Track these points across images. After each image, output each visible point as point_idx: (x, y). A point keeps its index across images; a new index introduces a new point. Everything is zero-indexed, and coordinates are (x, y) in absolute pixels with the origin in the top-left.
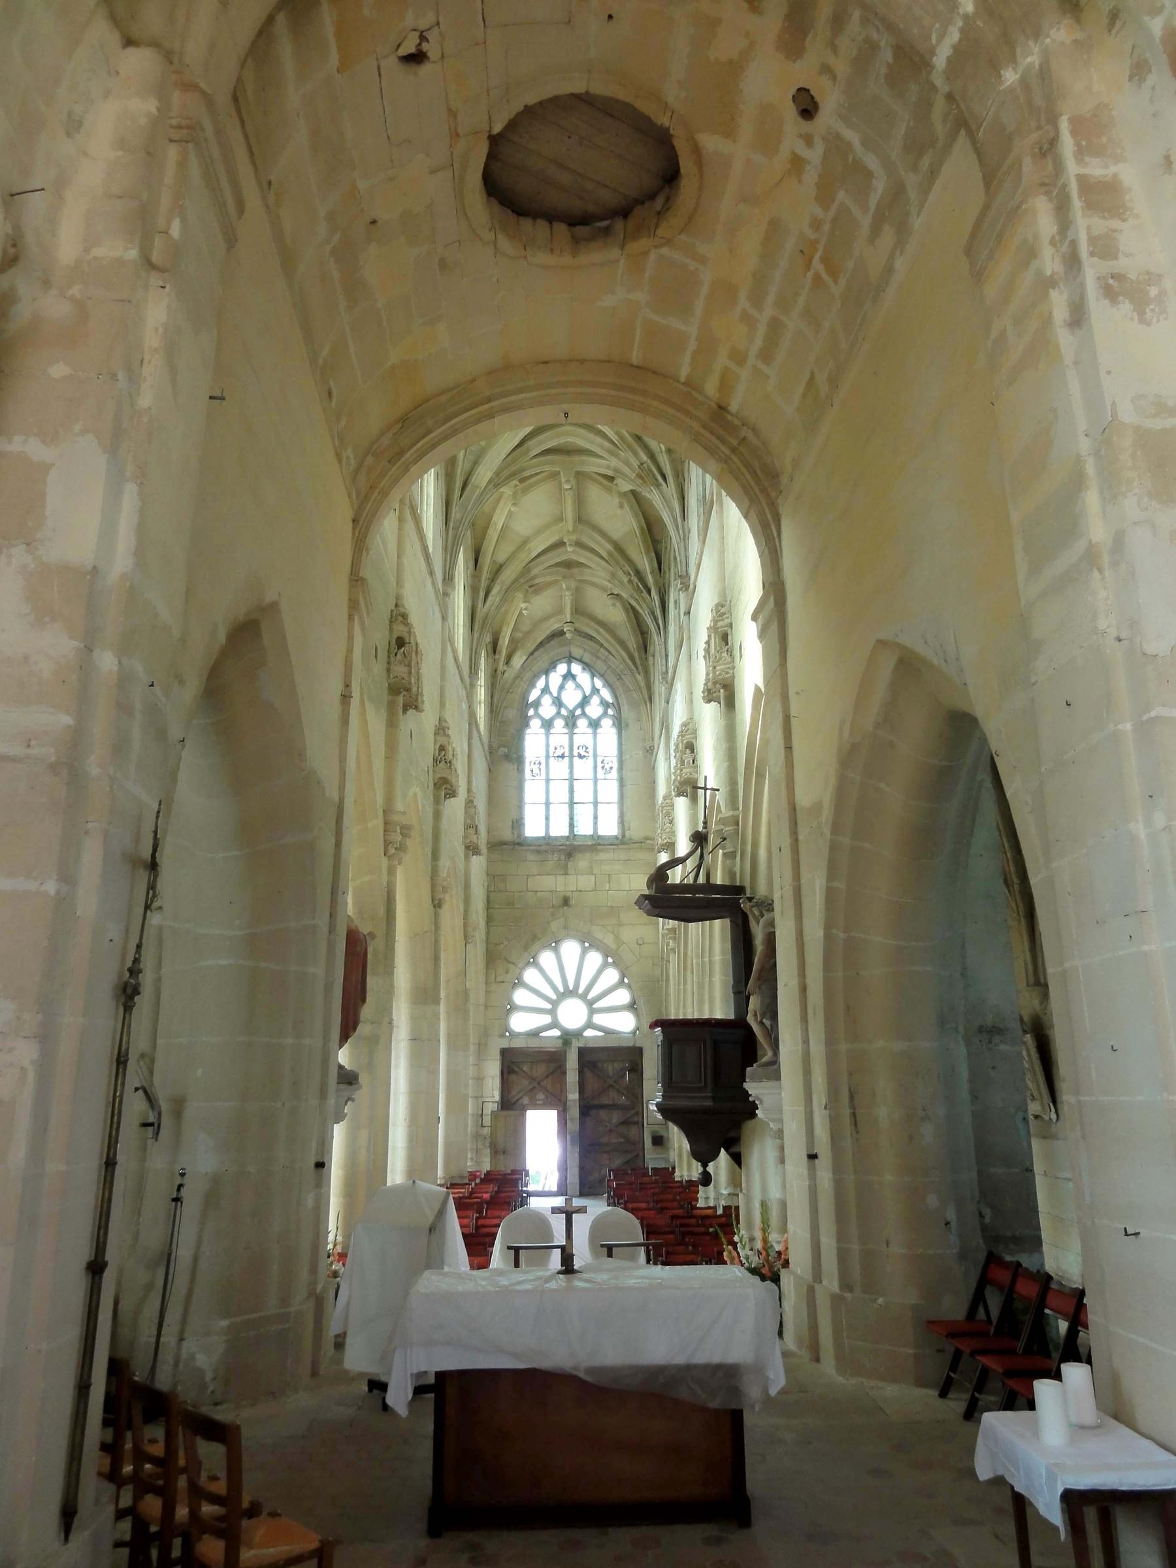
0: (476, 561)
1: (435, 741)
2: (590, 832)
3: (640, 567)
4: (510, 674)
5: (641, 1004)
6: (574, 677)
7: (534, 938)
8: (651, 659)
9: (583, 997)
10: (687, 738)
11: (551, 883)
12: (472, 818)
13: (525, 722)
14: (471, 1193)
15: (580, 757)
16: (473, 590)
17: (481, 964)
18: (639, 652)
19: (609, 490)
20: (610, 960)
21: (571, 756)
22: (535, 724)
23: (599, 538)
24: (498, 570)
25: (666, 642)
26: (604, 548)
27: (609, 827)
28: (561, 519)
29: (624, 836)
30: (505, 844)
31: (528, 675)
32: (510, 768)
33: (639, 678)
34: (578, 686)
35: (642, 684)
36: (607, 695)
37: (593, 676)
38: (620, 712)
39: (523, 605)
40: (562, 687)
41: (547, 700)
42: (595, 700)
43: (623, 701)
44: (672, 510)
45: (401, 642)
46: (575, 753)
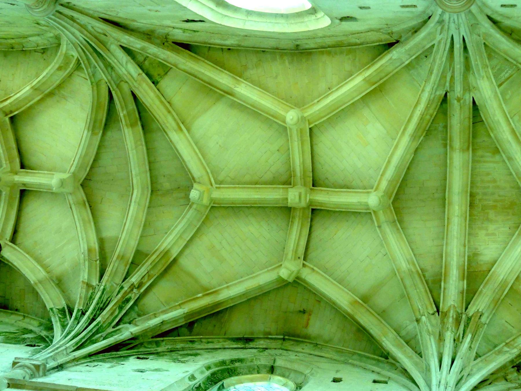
3: (150, 301)
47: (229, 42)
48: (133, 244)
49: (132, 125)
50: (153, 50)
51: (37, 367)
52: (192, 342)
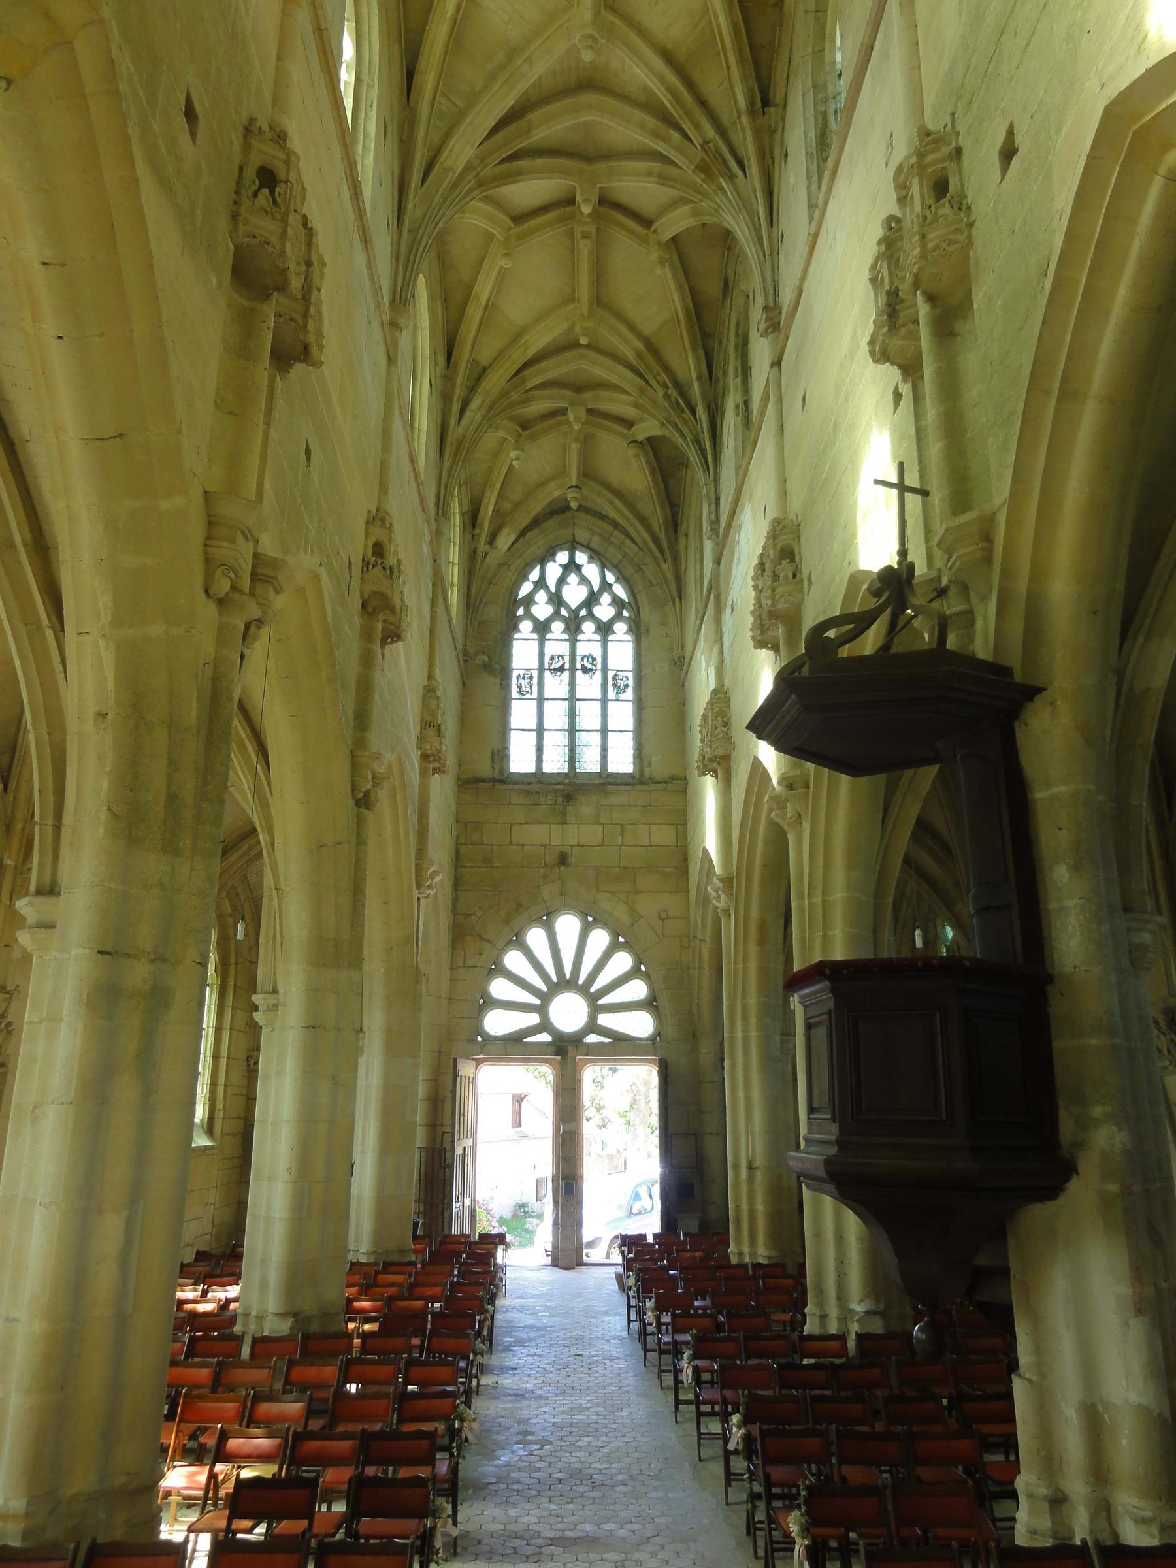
0: (449, 355)
1: (367, 533)
2: (596, 768)
3: (681, 374)
4: (492, 560)
5: (664, 1000)
6: (578, 568)
7: (520, 907)
8: (682, 540)
9: (584, 990)
11: (542, 835)
12: (433, 714)
13: (513, 625)
14: (412, 1286)
15: (585, 670)
16: (444, 397)
17: (445, 939)
18: (666, 528)
19: (643, 241)
20: (621, 940)
21: (573, 670)
22: (526, 626)
23: (624, 330)
24: (480, 374)
25: (716, 480)
26: (629, 347)
27: (622, 761)
28: (572, 299)
29: (642, 775)
30: (483, 780)
31: (519, 563)
32: (490, 681)
33: (665, 567)
34: (584, 580)
35: (670, 575)
36: (620, 591)
37: (603, 568)
39: (513, 454)
40: (562, 581)
41: (541, 597)
42: (606, 598)
43: (643, 598)
44: (753, 215)
45: (268, 178)
46: (579, 666)
47: (439, 309)
48: (630, 375)
49: (523, 382)
52: (721, 343)
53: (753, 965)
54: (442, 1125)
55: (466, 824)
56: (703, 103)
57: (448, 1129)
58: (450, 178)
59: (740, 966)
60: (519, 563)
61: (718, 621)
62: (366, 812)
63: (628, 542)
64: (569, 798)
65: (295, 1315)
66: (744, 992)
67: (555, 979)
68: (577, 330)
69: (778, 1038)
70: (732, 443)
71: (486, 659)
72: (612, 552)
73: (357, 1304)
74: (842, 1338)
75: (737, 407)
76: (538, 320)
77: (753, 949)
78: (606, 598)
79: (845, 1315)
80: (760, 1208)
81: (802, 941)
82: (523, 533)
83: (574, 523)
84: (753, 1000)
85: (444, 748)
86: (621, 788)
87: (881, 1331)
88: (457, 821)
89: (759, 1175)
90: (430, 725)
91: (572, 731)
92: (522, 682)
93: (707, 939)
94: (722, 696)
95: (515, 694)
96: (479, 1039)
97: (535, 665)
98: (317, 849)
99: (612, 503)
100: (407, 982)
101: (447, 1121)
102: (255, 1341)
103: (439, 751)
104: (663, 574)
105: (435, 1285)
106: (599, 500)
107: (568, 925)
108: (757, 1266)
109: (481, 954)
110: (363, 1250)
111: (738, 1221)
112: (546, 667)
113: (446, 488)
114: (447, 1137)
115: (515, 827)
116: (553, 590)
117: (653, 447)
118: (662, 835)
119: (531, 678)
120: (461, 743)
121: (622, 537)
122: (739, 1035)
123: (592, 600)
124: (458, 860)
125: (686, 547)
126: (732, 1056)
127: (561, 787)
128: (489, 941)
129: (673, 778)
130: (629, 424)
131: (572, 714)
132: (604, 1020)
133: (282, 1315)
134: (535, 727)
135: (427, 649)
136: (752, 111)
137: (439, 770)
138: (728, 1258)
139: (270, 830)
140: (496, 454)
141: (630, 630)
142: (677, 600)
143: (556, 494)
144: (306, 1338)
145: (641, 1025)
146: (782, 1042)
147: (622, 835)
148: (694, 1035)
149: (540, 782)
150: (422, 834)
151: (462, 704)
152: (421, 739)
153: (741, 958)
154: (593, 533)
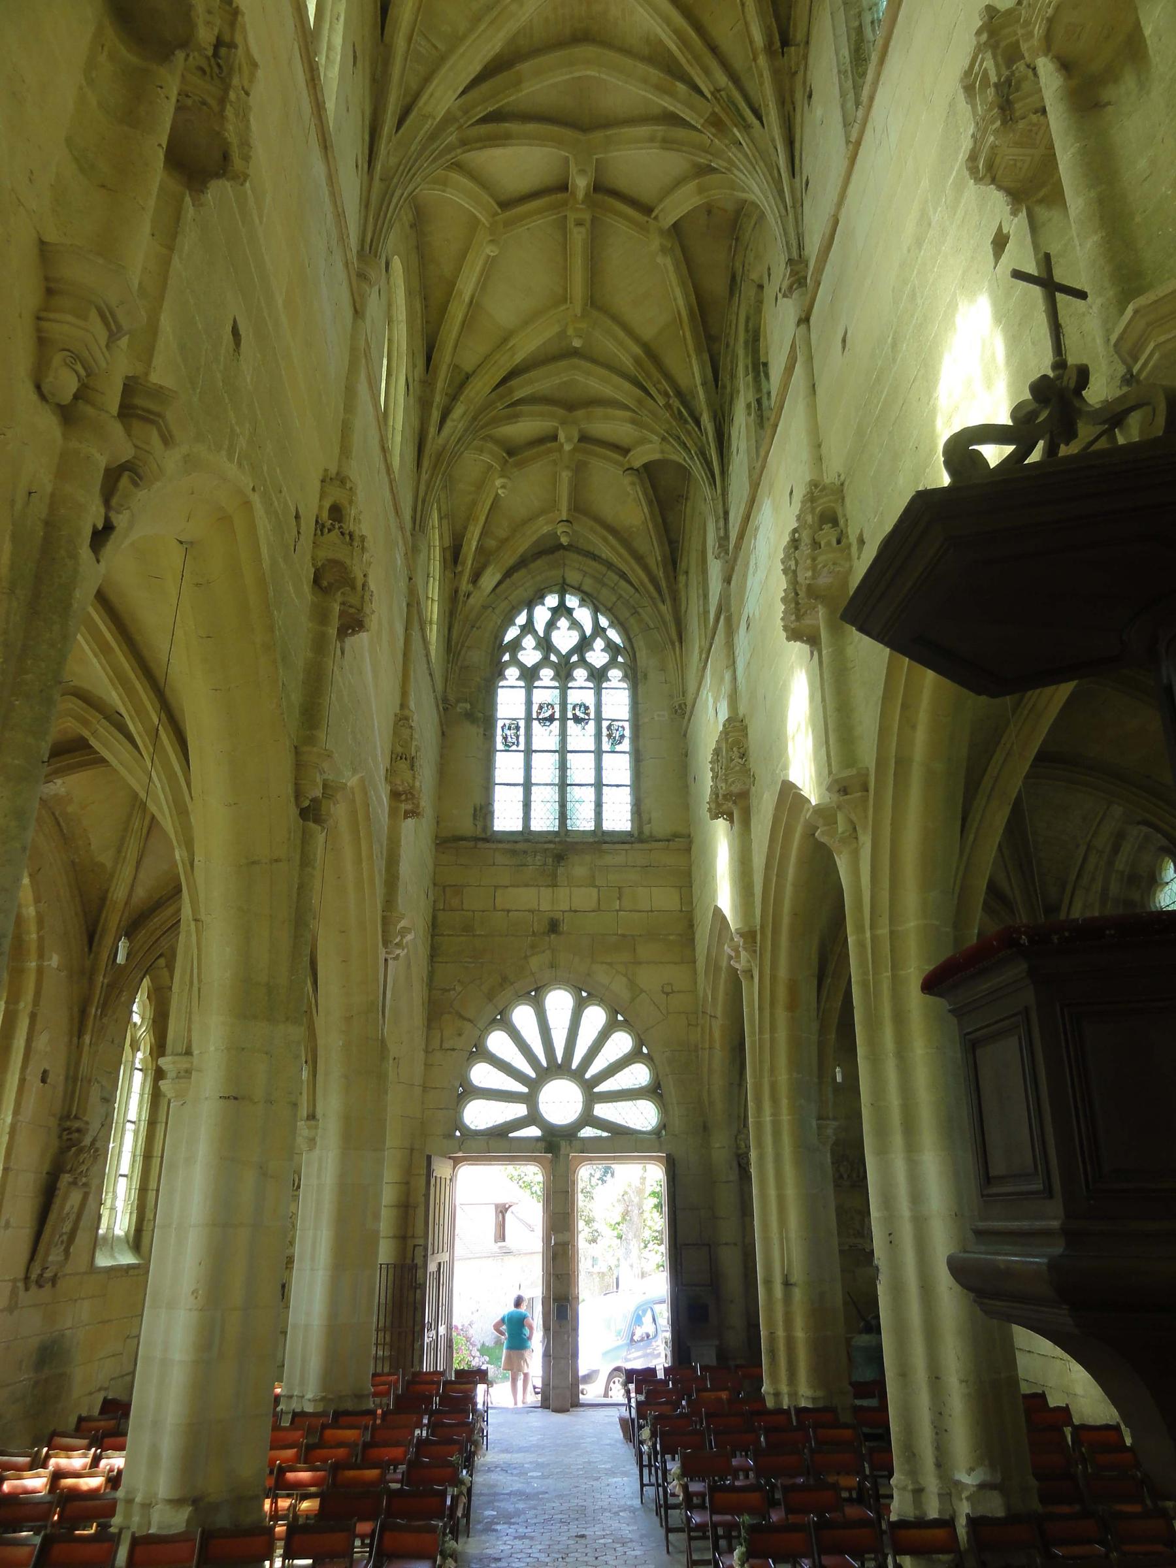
0: (429, 359)
1: (323, 495)
2: (590, 826)
3: (683, 382)
4: (476, 600)
6: (569, 612)
7: (504, 981)
8: (682, 579)
9: (577, 1076)
10: (822, 504)
11: (530, 899)
15: (577, 720)
17: (419, 1019)
18: (665, 567)
19: (643, 228)
20: (620, 1018)
21: (564, 720)
22: (512, 673)
23: (621, 334)
24: (461, 382)
25: (724, 494)
26: (626, 354)
27: (618, 818)
28: (565, 300)
29: (641, 832)
31: (504, 605)
32: (473, 731)
33: (663, 608)
34: (575, 625)
35: (669, 618)
36: (614, 635)
37: (596, 611)
38: (634, 658)
39: (498, 482)
40: (551, 625)
41: (529, 642)
42: (599, 644)
43: (640, 643)
44: (772, 168)
46: (570, 715)
47: (418, 306)
48: (627, 385)
49: (511, 391)
50: (437, 399)
51: (720, 546)
53: (782, 1035)
54: (413, 1237)
55: (444, 887)
56: (714, 49)
57: (421, 1242)
58: (428, 126)
59: (767, 1036)
60: (504, 605)
61: (730, 645)
62: (311, 825)
63: (623, 583)
64: (560, 858)
65: (195, 1502)
66: (772, 1070)
67: (544, 1064)
68: (570, 332)
69: (814, 1123)
70: (743, 446)
71: (468, 706)
72: (605, 595)
73: (290, 1476)
74: (948, 1523)
75: (749, 406)
76: (526, 323)
77: (782, 1015)
78: (599, 644)
79: (951, 1488)
80: (800, 1334)
81: (865, 985)
82: (508, 574)
83: (565, 564)
84: (783, 1077)
85: (417, 784)
86: (617, 846)
87: (1000, 1513)
88: (435, 885)
89: (798, 1294)
90: (402, 756)
91: (563, 785)
92: (508, 733)
93: (719, 1013)
94: (738, 724)
95: (499, 745)
96: (458, 1134)
97: (522, 715)
98: (248, 866)
99: (605, 540)
100: (370, 1061)
101: (419, 1231)
102: (135, 1542)
103: (412, 787)
104: (662, 617)
105: (397, 1444)
106: (592, 537)
107: (559, 1002)
108: (800, 1411)
109: (460, 1035)
110: (309, 1396)
111: (773, 1353)
112: (534, 716)
113: (424, 501)
114: (419, 1252)
115: (499, 892)
116: (541, 634)
117: (650, 473)
118: (664, 899)
119: (518, 728)
120: (439, 798)
121: (616, 578)
122: (767, 1118)
123: (584, 644)
124: (434, 927)
125: (687, 585)
126: (760, 1145)
127: (552, 846)
128: (469, 1020)
129: (676, 836)
130: (625, 451)
131: (563, 767)
132: (602, 1110)
133: (177, 1503)
134: (522, 781)
135: (400, 675)
136: (769, 49)
137: (413, 813)
138: (762, 1399)
139: (189, 844)
140: (480, 486)
141: (626, 677)
142: (677, 644)
143: (546, 529)
144: (208, 1536)
145: (642, 1116)
146: (819, 1127)
147: (619, 898)
148: (705, 1128)
149: (527, 841)
150: (391, 882)
151: (442, 756)
152: (391, 773)
153: (767, 1026)
154: (585, 574)
